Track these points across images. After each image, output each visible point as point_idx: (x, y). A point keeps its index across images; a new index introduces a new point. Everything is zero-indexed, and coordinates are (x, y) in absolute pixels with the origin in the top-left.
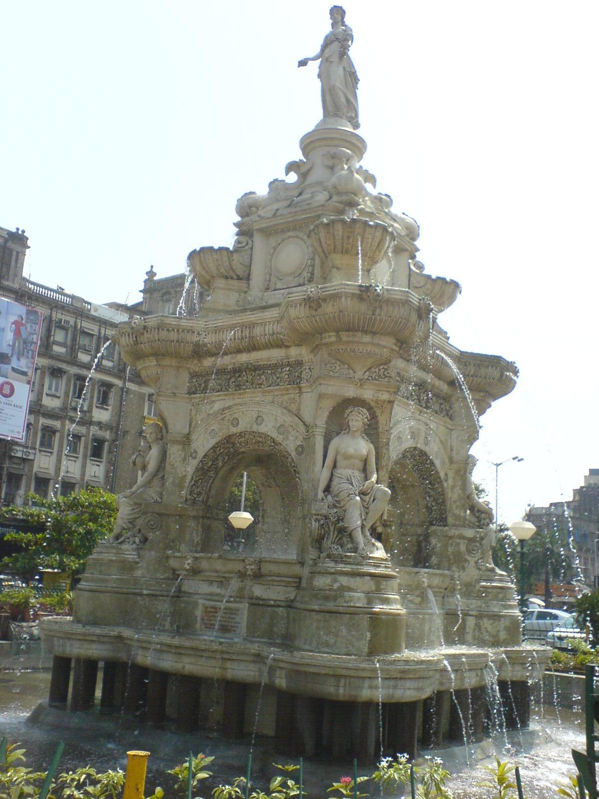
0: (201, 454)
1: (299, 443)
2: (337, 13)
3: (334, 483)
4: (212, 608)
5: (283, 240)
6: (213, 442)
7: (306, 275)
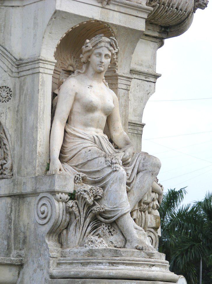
3: (69, 146)
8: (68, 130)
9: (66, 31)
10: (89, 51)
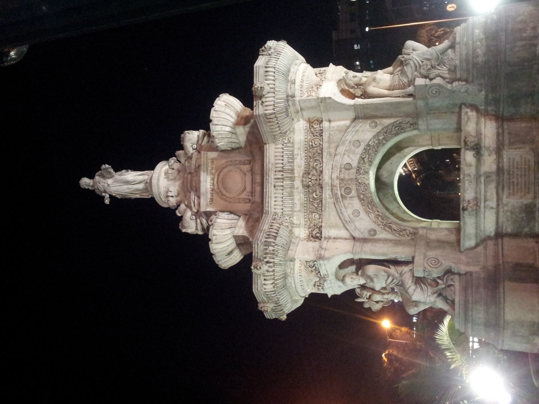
0: (374, 226)
1: (368, 126)
4: (509, 188)
6: (363, 215)
7: (246, 168)
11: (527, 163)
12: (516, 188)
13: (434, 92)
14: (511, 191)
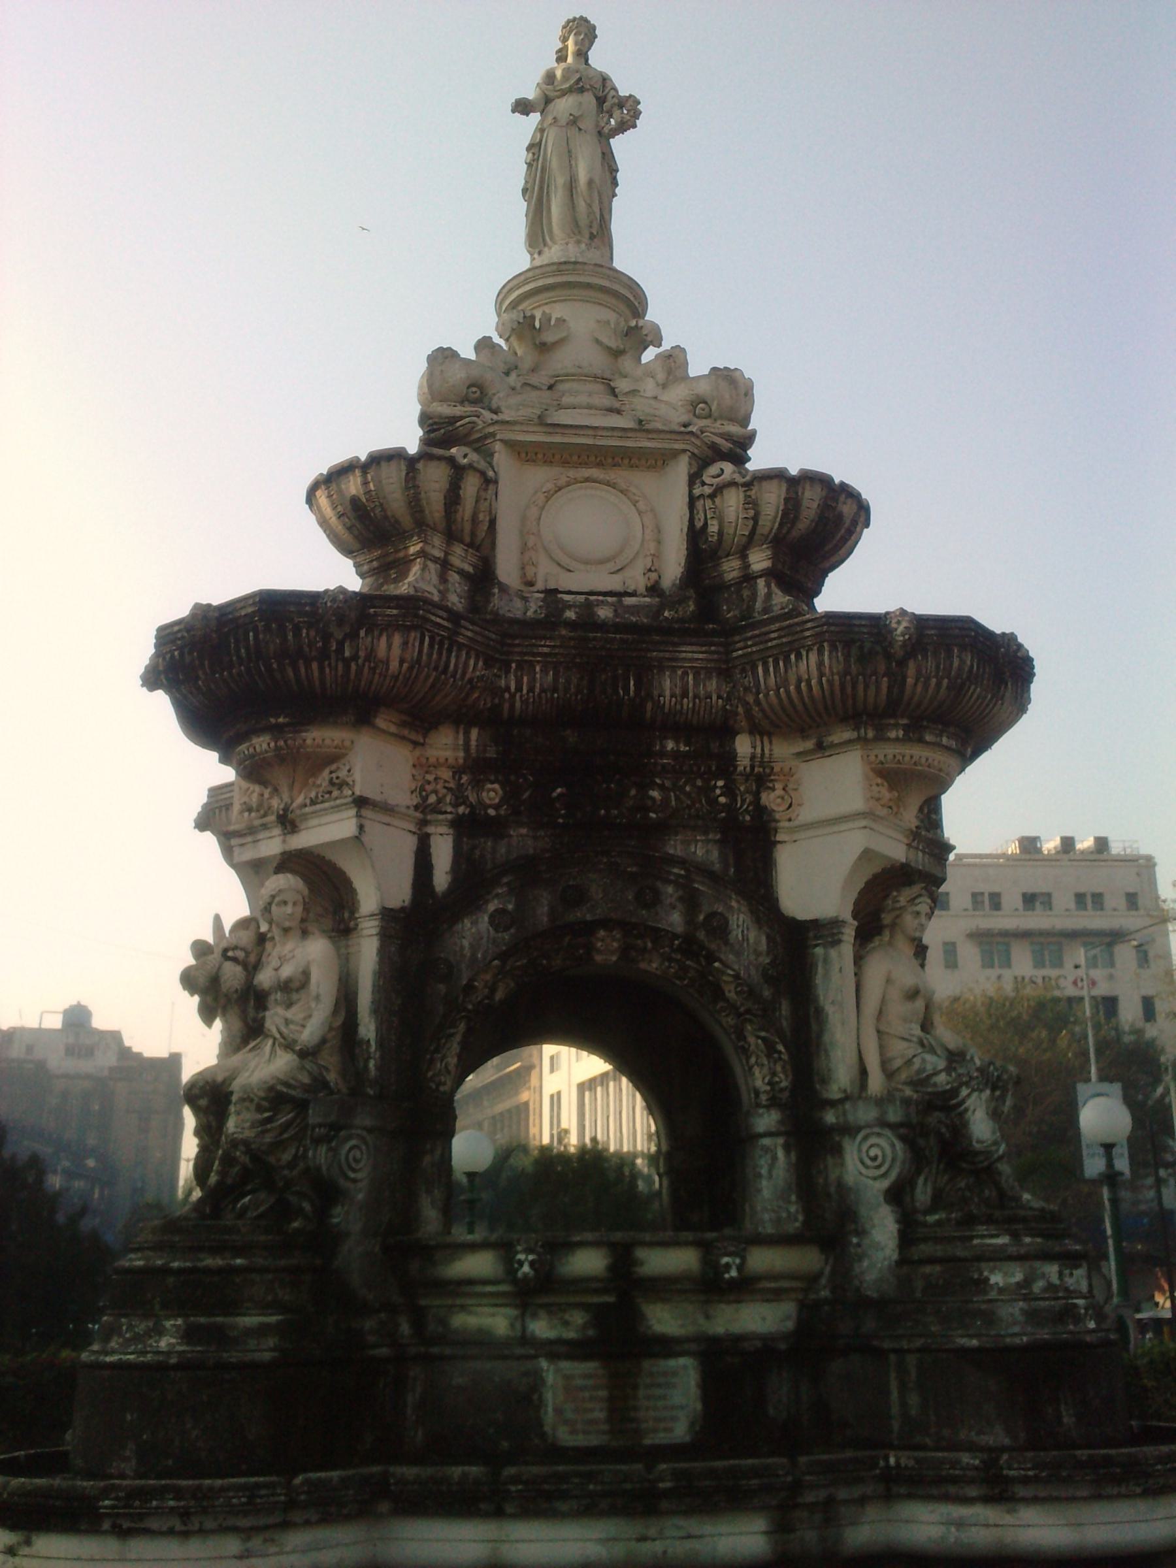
2: (583, 31)
5: (568, 484)
8: (882, 1028)
9: (865, 880)
10: (901, 908)
11: (662, 1425)
12: (587, 1394)
13: (873, 1152)
14: (579, 1382)
